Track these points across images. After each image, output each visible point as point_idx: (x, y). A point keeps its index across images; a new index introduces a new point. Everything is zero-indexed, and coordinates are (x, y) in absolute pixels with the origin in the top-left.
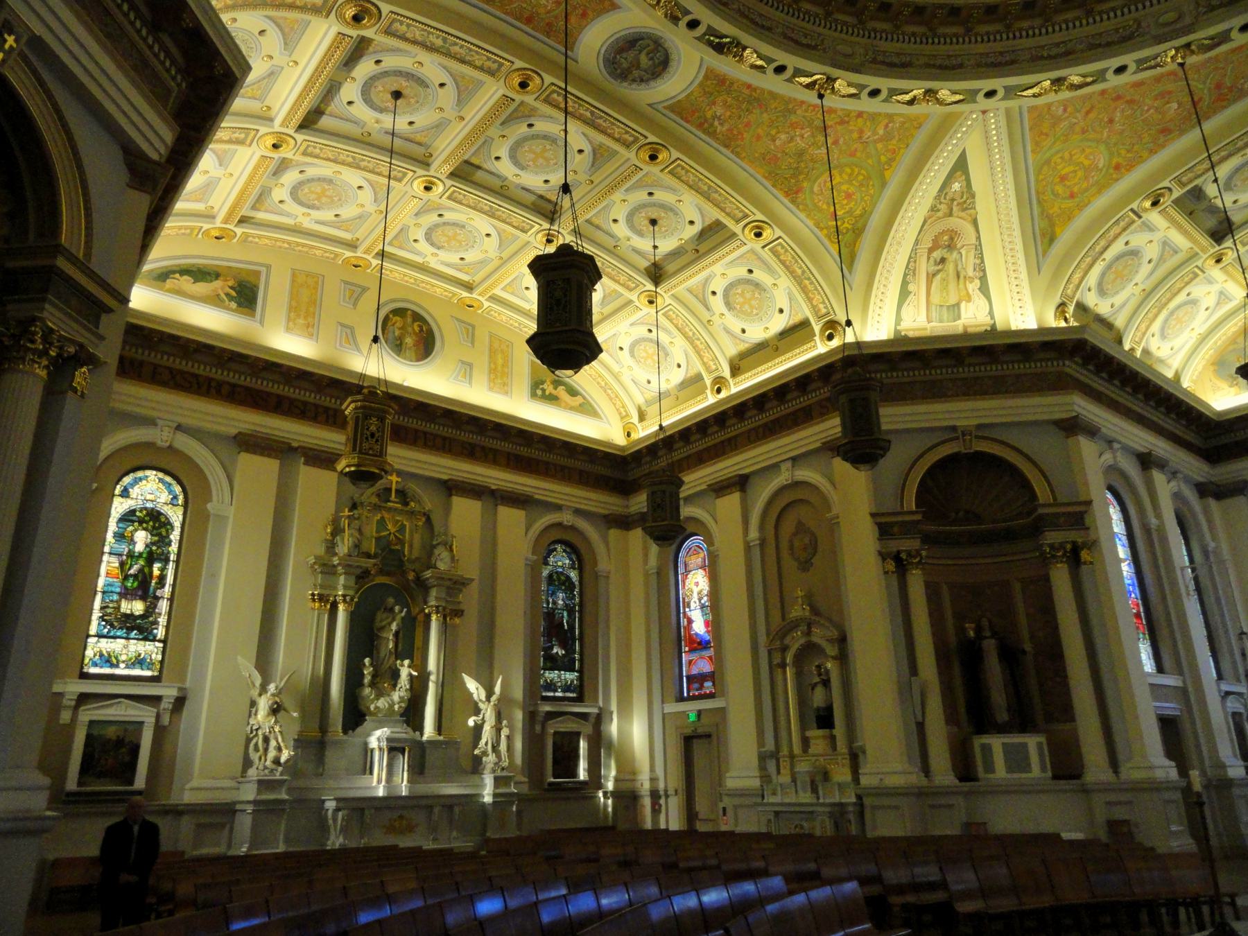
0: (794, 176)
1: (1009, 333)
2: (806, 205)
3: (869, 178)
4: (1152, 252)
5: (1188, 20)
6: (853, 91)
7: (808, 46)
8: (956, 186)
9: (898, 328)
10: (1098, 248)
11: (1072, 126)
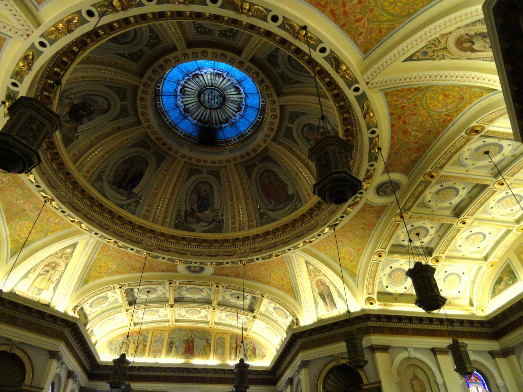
0: (15, 214)
1: (53, 310)
2: (12, 226)
3: (42, 231)
4: (111, 300)
5: (153, 248)
6: (57, 207)
7: (53, 187)
8: (68, 251)
9: (15, 288)
10: (98, 293)
11: (112, 254)
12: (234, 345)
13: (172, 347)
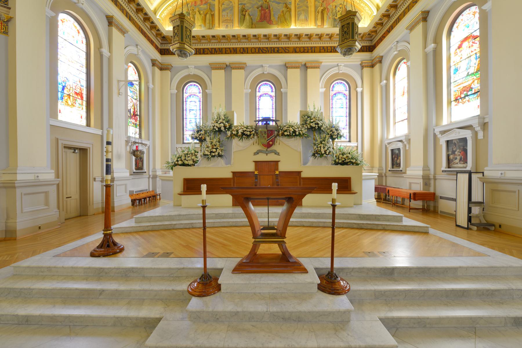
12: (320, 9)
13: (245, 15)
